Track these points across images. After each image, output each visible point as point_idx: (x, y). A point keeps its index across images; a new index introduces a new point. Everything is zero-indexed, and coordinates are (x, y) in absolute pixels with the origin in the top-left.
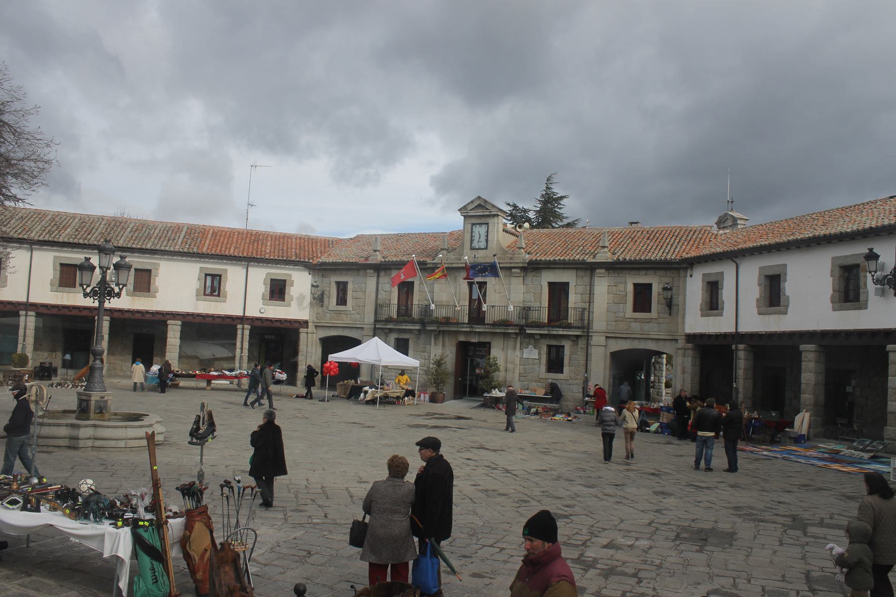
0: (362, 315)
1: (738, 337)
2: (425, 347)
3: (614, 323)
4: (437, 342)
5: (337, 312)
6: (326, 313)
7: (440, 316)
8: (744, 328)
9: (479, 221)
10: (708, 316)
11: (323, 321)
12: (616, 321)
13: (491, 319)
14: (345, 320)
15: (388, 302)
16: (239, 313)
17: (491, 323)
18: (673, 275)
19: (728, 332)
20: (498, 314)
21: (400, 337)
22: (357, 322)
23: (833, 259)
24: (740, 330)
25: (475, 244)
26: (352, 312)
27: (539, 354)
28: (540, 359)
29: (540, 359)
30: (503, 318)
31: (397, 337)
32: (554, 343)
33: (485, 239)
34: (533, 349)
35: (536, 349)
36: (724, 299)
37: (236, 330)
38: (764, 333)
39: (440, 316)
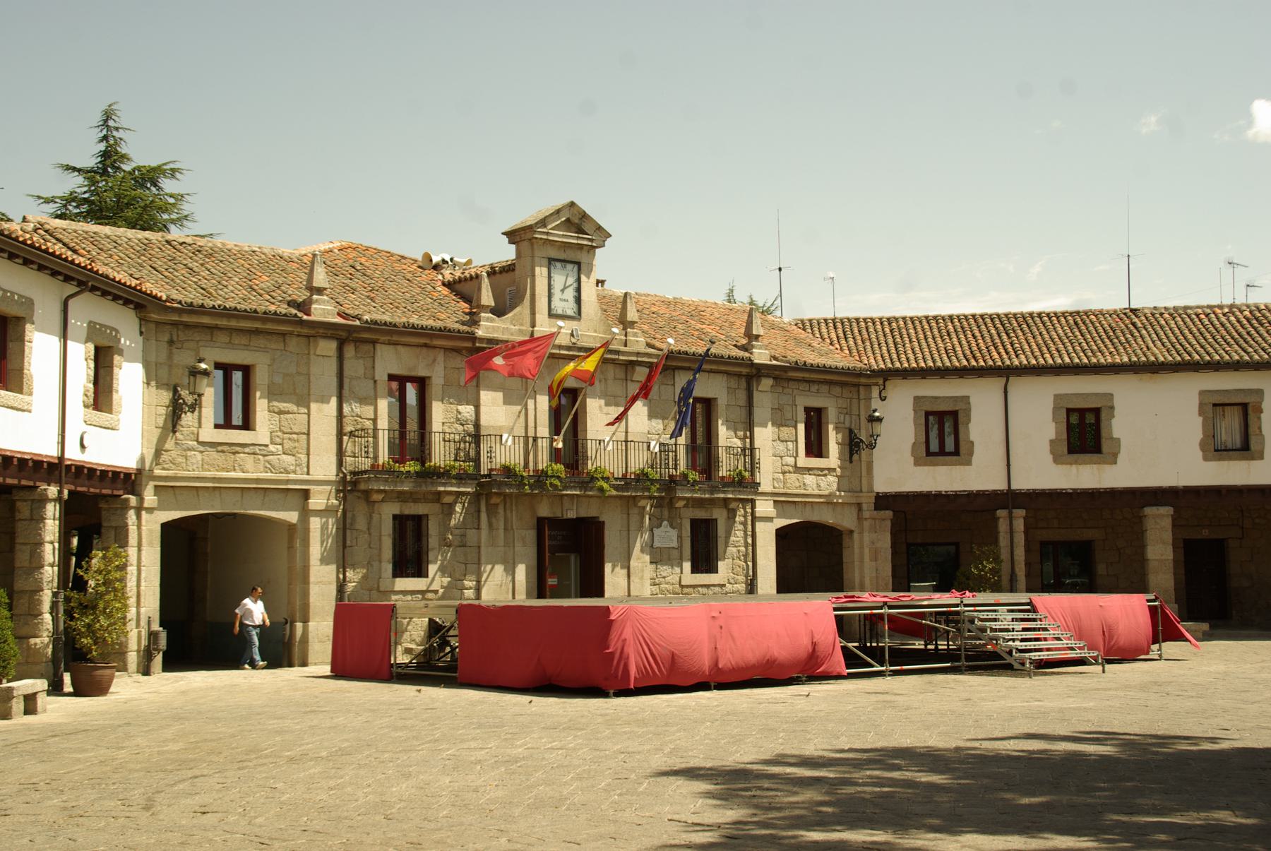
0: (303, 457)
1: (1010, 499)
2: (464, 535)
3: (781, 476)
4: (494, 520)
5: (225, 448)
6: (189, 450)
7: (512, 462)
8: (1022, 483)
9: (562, 256)
10: (925, 464)
11: (186, 473)
12: (784, 473)
13: (633, 465)
14: (250, 470)
15: (369, 424)
16: (48, 449)
17: (620, 476)
18: (851, 395)
19: (987, 491)
20: (616, 459)
21: (407, 512)
22: (292, 476)
23: (1202, 393)
24: (1014, 487)
25: (558, 306)
26: (272, 448)
27: (680, 537)
28: (680, 547)
29: (680, 547)
30: (503, 462)
31: (397, 512)
32: (701, 514)
33: (575, 297)
34: (669, 529)
35: (674, 528)
36: (974, 436)
37: (996, 520)
38: (1071, 491)
39: (512, 462)
